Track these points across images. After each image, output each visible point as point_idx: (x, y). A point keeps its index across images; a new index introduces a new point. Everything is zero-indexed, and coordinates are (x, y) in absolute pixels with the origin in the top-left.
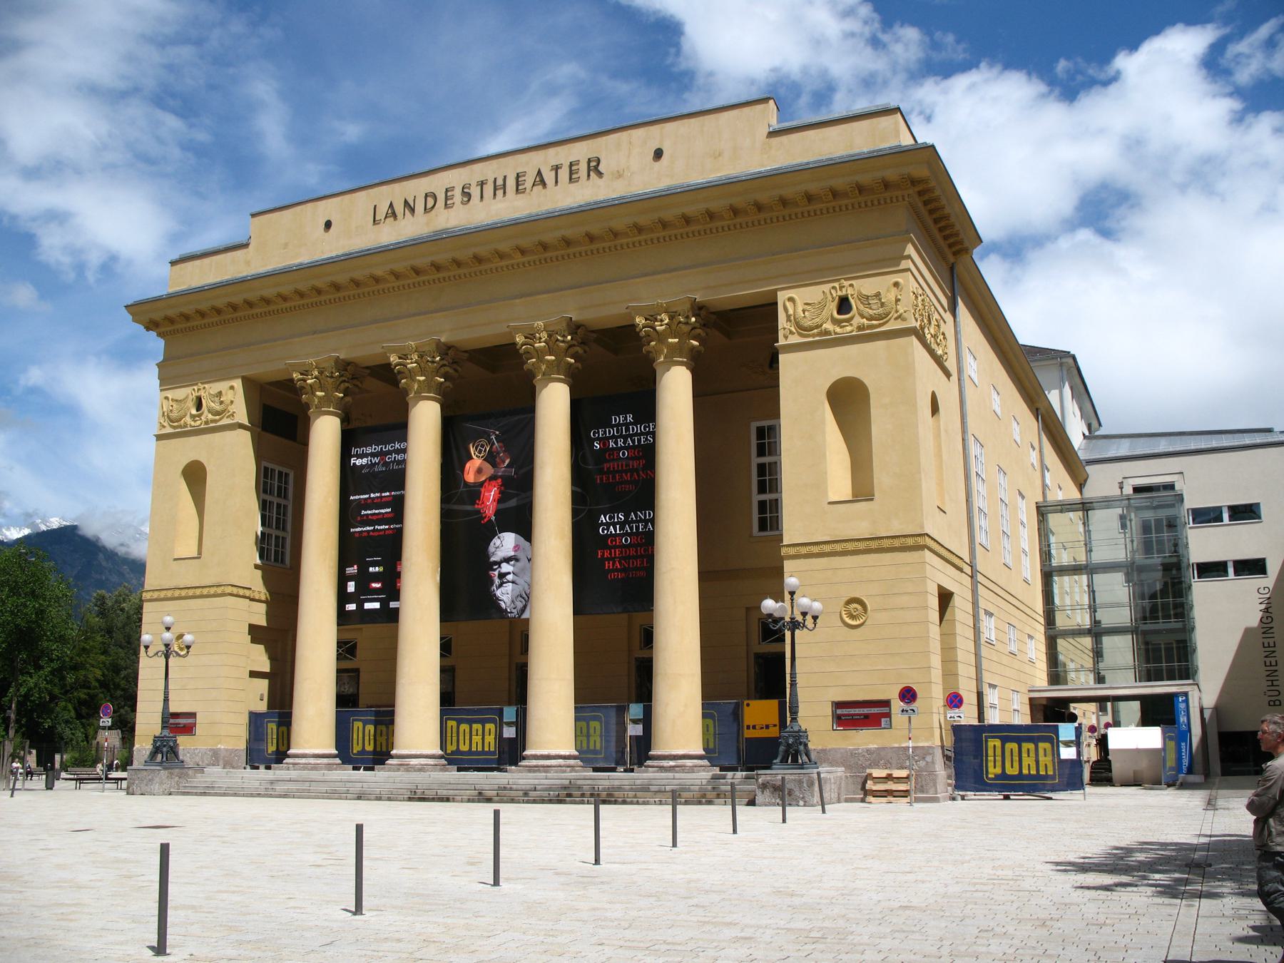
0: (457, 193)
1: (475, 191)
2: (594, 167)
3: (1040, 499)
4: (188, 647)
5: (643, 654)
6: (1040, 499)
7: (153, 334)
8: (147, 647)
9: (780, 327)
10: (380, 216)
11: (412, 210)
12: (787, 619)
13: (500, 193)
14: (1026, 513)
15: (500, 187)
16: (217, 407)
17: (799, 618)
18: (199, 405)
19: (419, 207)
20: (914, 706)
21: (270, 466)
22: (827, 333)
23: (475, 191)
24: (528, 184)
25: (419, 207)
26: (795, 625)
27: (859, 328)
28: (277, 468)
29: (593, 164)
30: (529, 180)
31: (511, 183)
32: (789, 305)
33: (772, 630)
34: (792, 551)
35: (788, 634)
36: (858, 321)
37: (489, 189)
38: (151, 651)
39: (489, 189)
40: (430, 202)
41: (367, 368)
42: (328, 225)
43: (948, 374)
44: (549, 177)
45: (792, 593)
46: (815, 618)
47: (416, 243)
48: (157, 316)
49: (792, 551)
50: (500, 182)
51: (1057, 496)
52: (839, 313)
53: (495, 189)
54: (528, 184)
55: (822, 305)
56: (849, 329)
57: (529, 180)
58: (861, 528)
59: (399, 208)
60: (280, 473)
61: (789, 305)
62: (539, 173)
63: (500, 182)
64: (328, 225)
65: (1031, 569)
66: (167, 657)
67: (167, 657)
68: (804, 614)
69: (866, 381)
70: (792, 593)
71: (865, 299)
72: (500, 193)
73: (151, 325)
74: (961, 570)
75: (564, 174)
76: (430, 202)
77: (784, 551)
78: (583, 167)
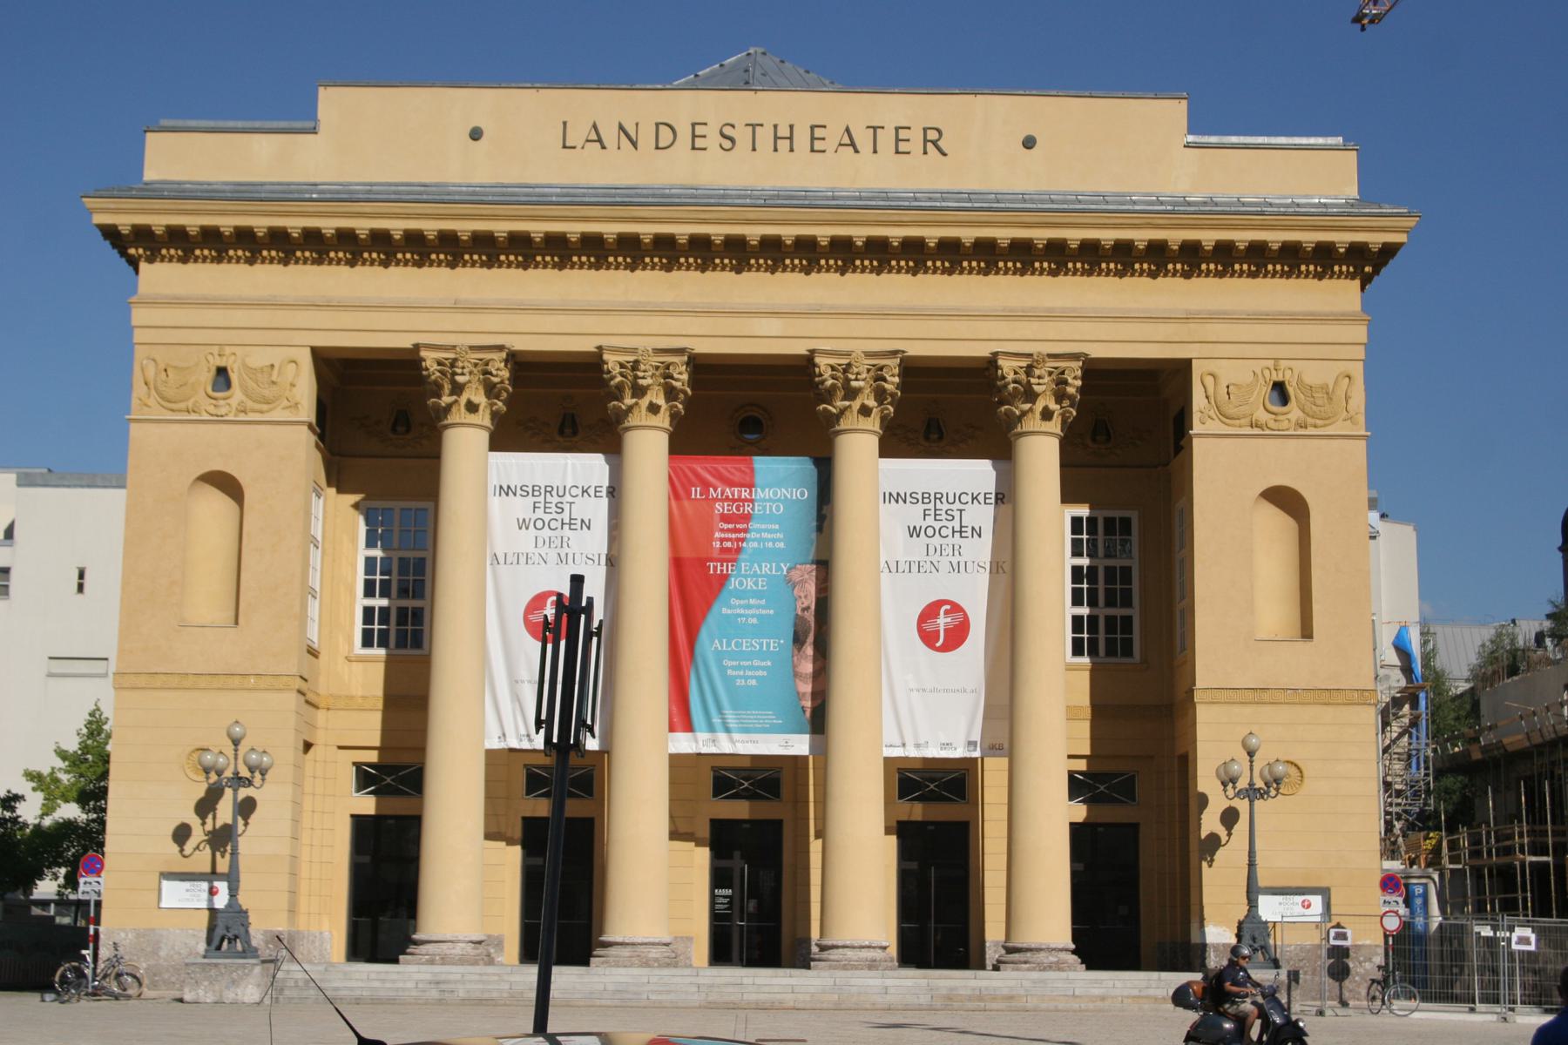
0: (712, 132)
1: (742, 135)
2: (933, 141)
9: (1195, 408)
13: (783, 145)
15: (784, 138)
19: (646, 138)
23: (742, 135)
24: (830, 145)
25: (646, 138)
29: (932, 135)
30: (834, 135)
31: (802, 138)
32: (1209, 381)
37: (765, 136)
39: (765, 136)
40: (665, 134)
42: (476, 134)
44: (863, 139)
53: (776, 138)
54: (830, 145)
56: (1285, 424)
57: (834, 135)
59: (609, 134)
61: (1209, 381)
64: (476, 134)
72: (783, 145)
75: (887, 139)
78: (916, 137)
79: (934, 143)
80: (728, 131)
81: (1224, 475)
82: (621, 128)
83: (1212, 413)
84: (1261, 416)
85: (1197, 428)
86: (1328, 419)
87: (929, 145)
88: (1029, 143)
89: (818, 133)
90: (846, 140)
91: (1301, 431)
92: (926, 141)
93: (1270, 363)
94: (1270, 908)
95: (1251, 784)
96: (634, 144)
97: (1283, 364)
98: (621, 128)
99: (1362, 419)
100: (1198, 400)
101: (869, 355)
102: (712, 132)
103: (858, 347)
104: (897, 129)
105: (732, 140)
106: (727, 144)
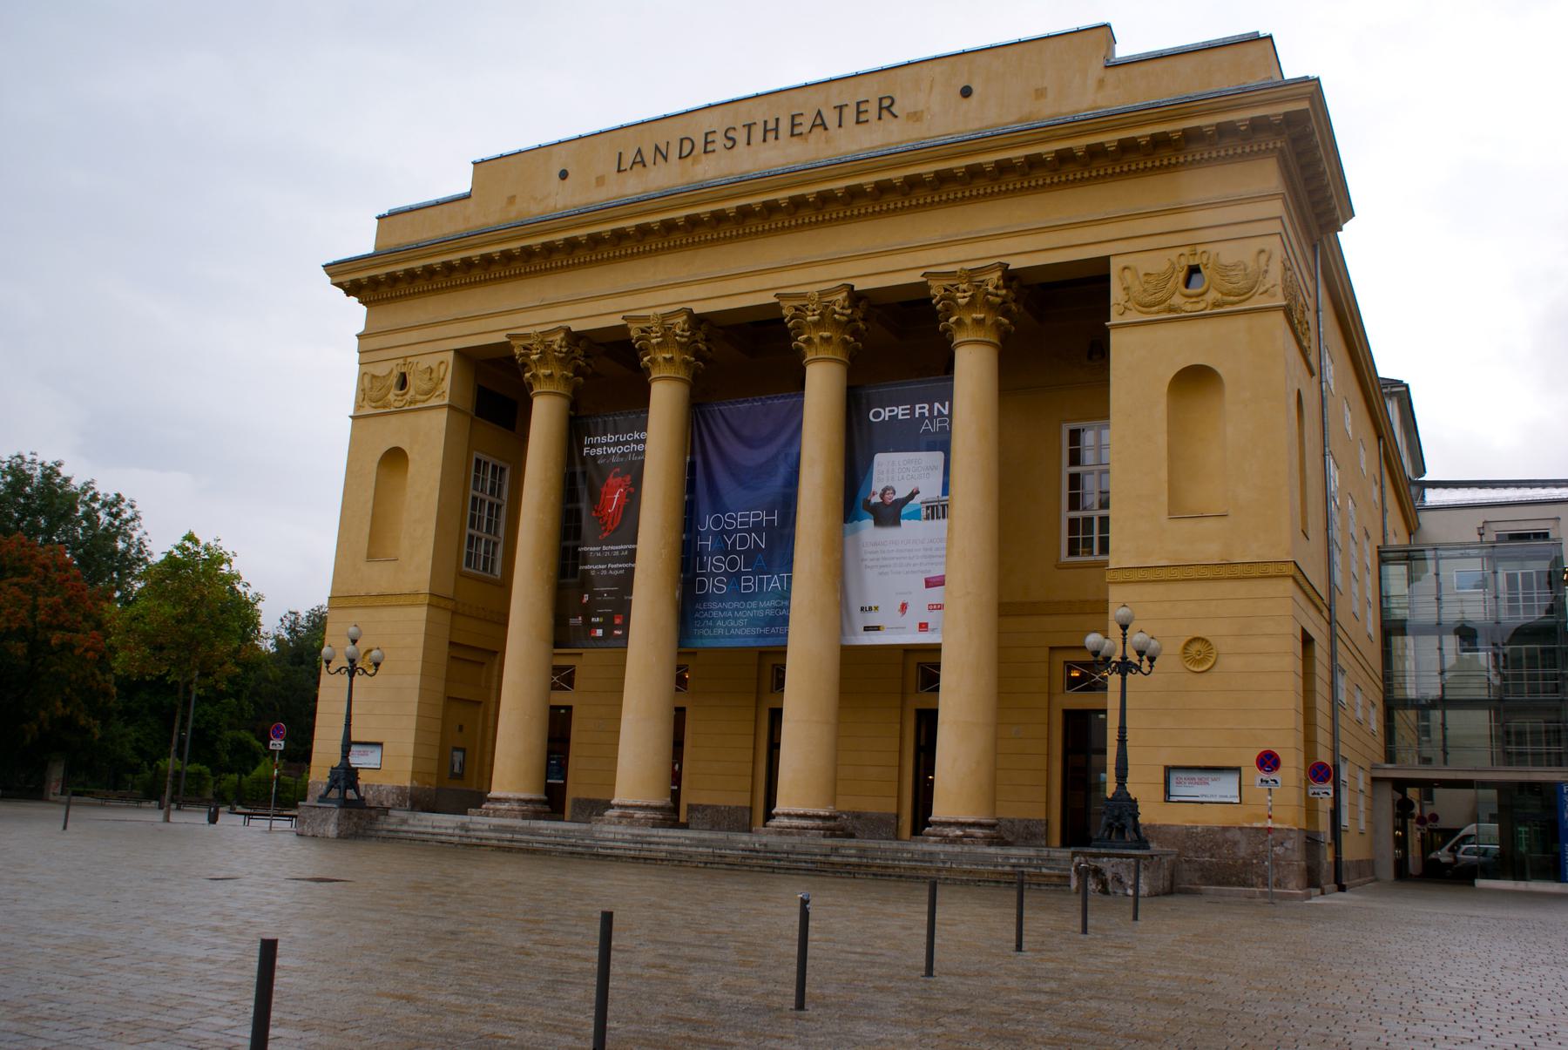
0: (719, 140)
1: (741, 136)
3: (1380, 543)
4: (377, 665)
5: (922, 701)
6: (1380, 543)
7: (354, 300)
8: (328, 662)
9: (1113, 301)
10: (626, 165)
11: (666, 158)
12: (1116, 658)
14: (1371, 559)
15: (771, 131)
16: (426, 386)
17: (1133, 657)
18: (403, 382)
19: (674, 154)
20: (1274, 776)
21: (484, 457)
22: (1171, 310)
23: (741, 136)
25: (674, 154)
26: (1125, 667)
27: (1216, 305)
28: (492, 461)
29: (886, 103)
30: (806, 123)
31: (785, 126)
33: (1090, 672)
34: (1120, 576)
35: (1114, 680)
36: (1213, 295)
37: (758, 133)
38: (333, 667)
39: (758, 133)
41: (602, 344)
42: (564, 175)
43: (1312, 374)
44: (831, 118)
45: (1124, 627)
46: (1152, 659)
47: (668, 197)
48: (363, 275)
49: (1120, 576)
50: (771, 125)
51: (1393, 541)
52: (1187, 286)
53: (766, 131)
54: (805, 129)
55: (1167, 277)
56: (1202, 305)
58: (1211, 551)
59: (649, 154)
60: (494, 467)
63: (771, 125)
64: (564, 175)
65: (1372, 626)
66: (352, 675)
67: (352, 675)
68: (1140, 653)
69: (1220, 370)
70: (1124, 627)
71: (1224, 270)
72: (771, 136)
73: (352, 289)
74: (1321, 612)
75: (849, 115)
76: (687, 147)
77: (1109, 576)
78: (873, 108)
80: (730, 134)
81: (1140, 359)
82: (657, 148)
83: (1129, 305)
84: (1177, 300)
85: (1115, 319)
86: (1247, 293)
87: (885, 113)
88: (966, 92)
91: (1217, 313)
92: (881, 109)
93: (1185, 250)
94: (356, 760)
95: (1124, 658)
96: (666, 158)
97: (1200, 249)
98: (657, 148)
99: (1279, 290)
100: (1116, 294)
101: (822, 294)
102: (719, 140)
103: (812, 289)
104: (858, 104)
106: (729, 144)
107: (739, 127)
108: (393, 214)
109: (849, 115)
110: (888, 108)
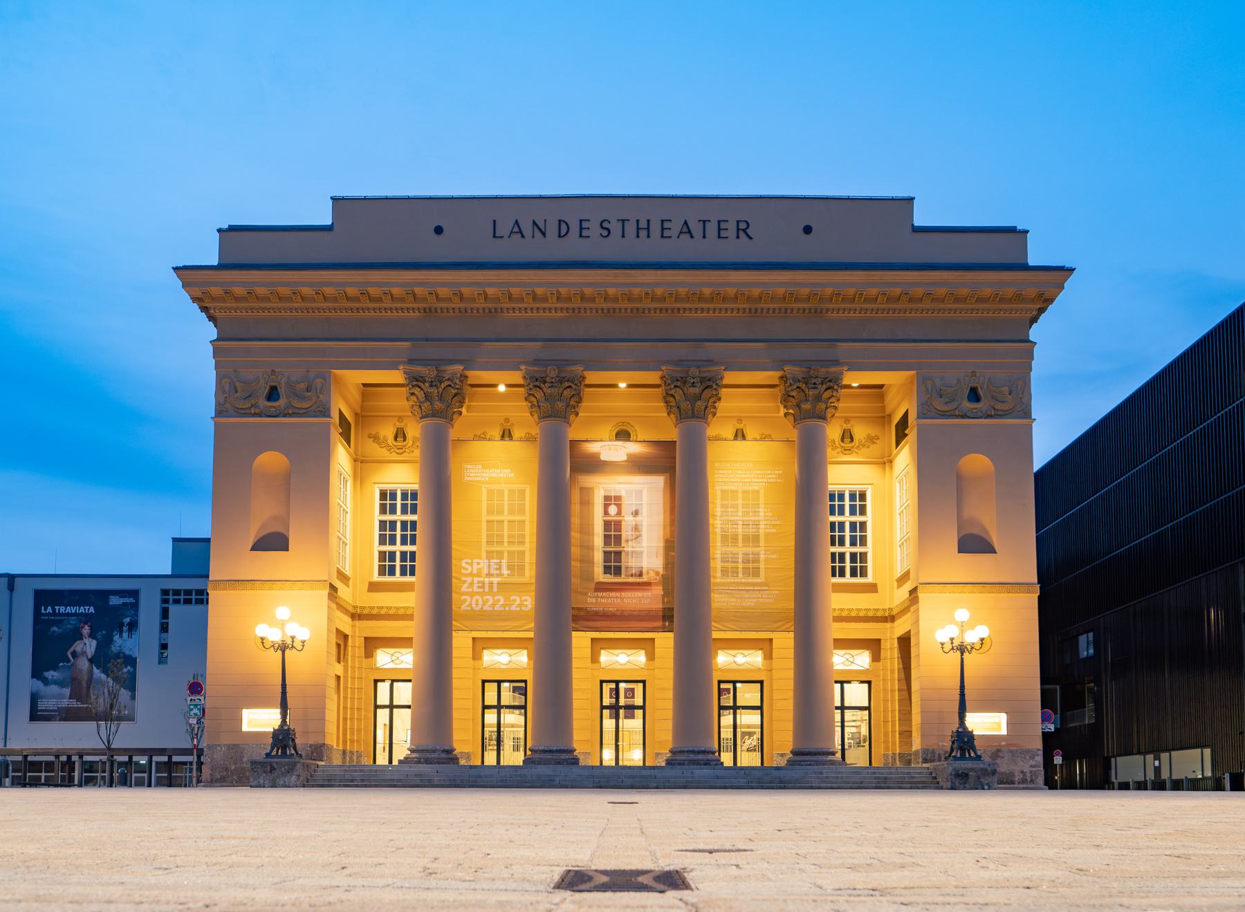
1: (616, 228)
10: (503, 230)
11: (544, 234)
13: (643, 233)
15: (644, 229)
23: (616, 228)
25: (552, 230)
29: (743, 226)
30: (676, 227)
37: (631, 228)
39: (631, 228)
44: (696, 229)
59: (527, 227)
62: (686, 223)
63: (643, 224)
75: (712, 229)
79: (744, 230)
82: (534, 223)
87: (741, 233)
89: (666, 225)
90: (685, 229)
92: (738, 229)
96: (544, 234)
105: (608, 230)
106: (605, 233)
107: (614, 221)
108: (232, 229)
109: (712, 229)
110: (744, 230)
